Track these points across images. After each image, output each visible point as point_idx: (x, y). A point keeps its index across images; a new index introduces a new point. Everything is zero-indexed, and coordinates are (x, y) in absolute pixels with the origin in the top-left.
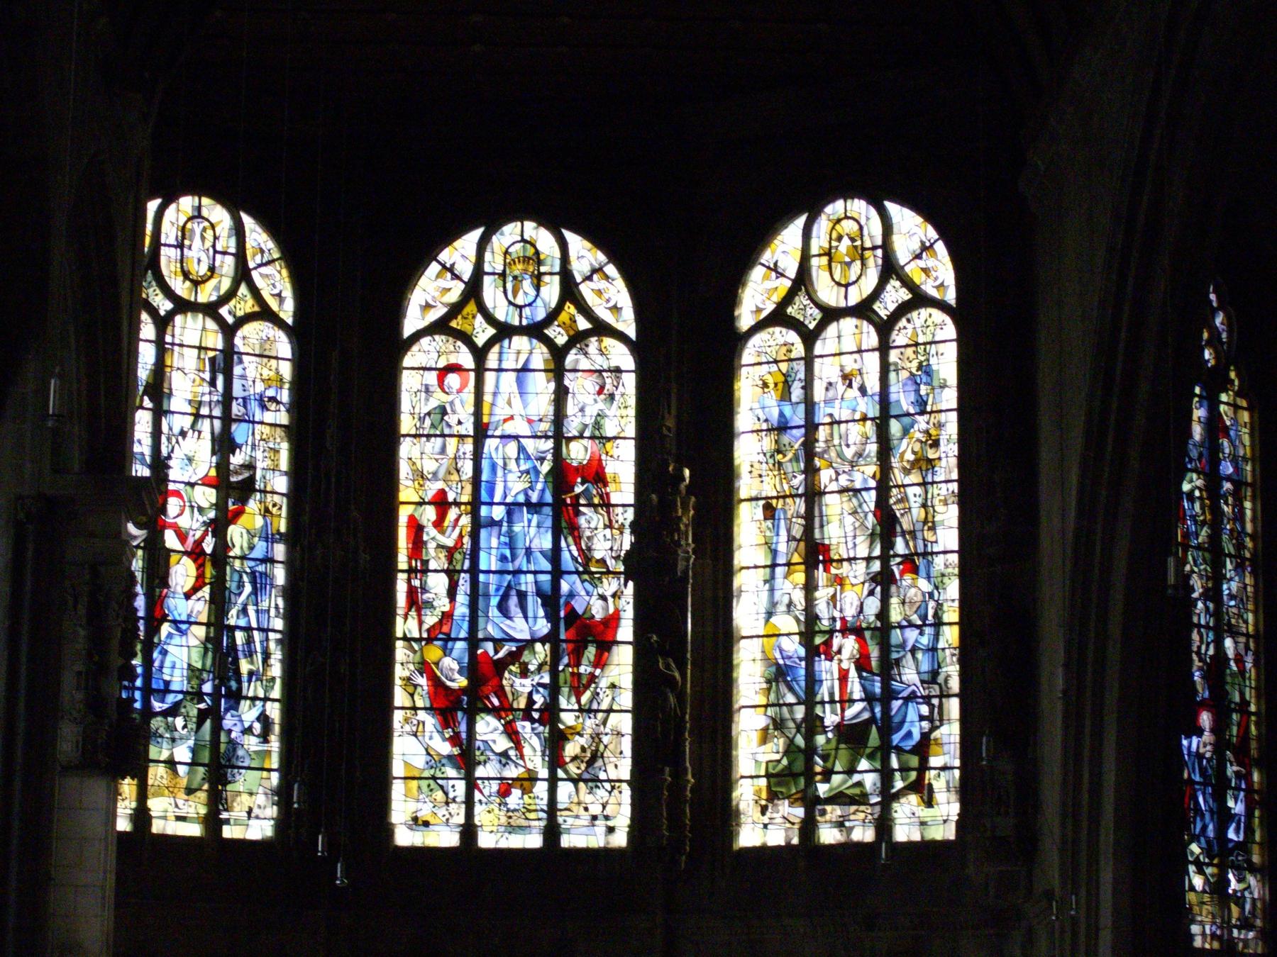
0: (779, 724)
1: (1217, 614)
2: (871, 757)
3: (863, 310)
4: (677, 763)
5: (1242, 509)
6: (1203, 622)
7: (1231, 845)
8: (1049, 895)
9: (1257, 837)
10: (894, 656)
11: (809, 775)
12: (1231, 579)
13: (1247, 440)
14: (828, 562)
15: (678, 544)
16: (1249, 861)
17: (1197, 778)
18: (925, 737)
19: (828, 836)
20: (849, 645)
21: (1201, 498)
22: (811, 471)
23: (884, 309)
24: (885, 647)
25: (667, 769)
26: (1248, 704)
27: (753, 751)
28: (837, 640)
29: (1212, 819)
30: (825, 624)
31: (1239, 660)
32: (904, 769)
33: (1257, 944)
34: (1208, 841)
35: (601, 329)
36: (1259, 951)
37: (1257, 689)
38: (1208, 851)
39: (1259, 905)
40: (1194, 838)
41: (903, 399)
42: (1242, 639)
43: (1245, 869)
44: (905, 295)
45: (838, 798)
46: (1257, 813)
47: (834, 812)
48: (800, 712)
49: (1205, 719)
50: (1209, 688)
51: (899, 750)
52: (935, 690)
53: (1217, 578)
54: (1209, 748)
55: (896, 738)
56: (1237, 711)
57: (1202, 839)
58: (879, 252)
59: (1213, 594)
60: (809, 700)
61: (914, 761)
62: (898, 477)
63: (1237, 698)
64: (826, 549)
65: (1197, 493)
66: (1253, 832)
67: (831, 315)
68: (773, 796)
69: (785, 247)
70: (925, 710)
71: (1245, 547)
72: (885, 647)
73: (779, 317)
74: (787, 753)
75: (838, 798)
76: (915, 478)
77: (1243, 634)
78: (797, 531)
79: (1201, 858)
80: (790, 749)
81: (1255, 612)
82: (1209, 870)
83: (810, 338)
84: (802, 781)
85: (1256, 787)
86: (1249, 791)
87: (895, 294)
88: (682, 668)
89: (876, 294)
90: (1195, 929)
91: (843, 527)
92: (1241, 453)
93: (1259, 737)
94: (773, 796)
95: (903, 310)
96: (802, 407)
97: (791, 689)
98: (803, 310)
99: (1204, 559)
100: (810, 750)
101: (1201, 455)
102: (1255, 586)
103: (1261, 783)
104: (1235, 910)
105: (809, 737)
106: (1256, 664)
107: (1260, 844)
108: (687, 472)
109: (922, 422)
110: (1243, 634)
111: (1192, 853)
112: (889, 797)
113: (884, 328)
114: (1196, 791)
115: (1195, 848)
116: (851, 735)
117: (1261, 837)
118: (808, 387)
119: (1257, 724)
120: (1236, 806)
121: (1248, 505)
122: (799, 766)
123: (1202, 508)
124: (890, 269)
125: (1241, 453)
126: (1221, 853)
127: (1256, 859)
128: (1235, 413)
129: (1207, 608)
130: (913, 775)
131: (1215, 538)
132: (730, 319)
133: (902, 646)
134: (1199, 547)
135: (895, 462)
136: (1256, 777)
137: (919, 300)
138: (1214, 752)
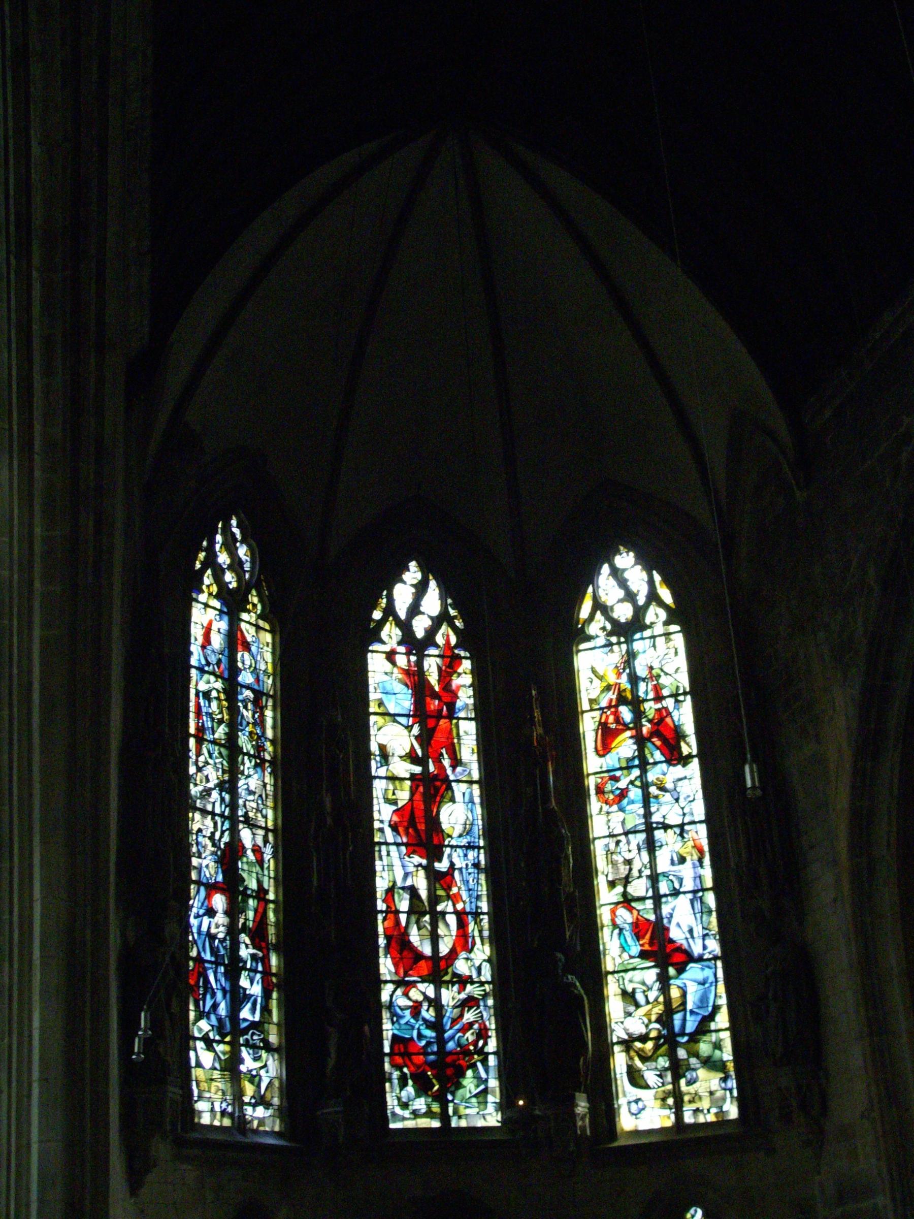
5: (262, 716)
6: (218, 811)
7: (244, 1025)
9: (275, 1018)
12: (249, 776)
13: (269, 657)
16: (265, 1041)
17: (207, 956)
21: (218, 698)
26: (267, 892)
29: (224, 997)
33: (274, 1122)
34: (220, 1020)
36: (277, 1129)
37: (275, 879)
38: (220, 1028)
39: (276, 1083)
40: (201, 1015)
42: (261, 832)
43: (262, 1048)
46: (275, 995)
50: (223, 872)
54: (222, 929)
56: (254, 898)
57: (213, 1017)
59: (229, 785)
65: (214, 694)
66: (270, 1012)
71: (264, 750)
77: (260, 827)
79: (211, 1035)
81: (275, 809)
82: (220, 1048)
85: (274, 970)
86: (266, 973)
90: (201, 1106)
92: (262, 667)
93: (277, 924)
99: (220, 753)
101: (219, 662)
102: (275, 785)
103: (278, 967)
106: (275, 855)
107: (278, 1025)
110: (260, 827)
111: (200, 1030)
114: (205, 969)
115: (204, 1025)
117: (279, 1017)
119: (276, 911)
121: (269, 713)
123: (220, 707)
125: (263, 667)
126: (231, 1030)
127: (273, 1039)
128: (257, 632)
129: (223, 800)
134: (214, 742)
136: (274, 960)
138: (227, 934)
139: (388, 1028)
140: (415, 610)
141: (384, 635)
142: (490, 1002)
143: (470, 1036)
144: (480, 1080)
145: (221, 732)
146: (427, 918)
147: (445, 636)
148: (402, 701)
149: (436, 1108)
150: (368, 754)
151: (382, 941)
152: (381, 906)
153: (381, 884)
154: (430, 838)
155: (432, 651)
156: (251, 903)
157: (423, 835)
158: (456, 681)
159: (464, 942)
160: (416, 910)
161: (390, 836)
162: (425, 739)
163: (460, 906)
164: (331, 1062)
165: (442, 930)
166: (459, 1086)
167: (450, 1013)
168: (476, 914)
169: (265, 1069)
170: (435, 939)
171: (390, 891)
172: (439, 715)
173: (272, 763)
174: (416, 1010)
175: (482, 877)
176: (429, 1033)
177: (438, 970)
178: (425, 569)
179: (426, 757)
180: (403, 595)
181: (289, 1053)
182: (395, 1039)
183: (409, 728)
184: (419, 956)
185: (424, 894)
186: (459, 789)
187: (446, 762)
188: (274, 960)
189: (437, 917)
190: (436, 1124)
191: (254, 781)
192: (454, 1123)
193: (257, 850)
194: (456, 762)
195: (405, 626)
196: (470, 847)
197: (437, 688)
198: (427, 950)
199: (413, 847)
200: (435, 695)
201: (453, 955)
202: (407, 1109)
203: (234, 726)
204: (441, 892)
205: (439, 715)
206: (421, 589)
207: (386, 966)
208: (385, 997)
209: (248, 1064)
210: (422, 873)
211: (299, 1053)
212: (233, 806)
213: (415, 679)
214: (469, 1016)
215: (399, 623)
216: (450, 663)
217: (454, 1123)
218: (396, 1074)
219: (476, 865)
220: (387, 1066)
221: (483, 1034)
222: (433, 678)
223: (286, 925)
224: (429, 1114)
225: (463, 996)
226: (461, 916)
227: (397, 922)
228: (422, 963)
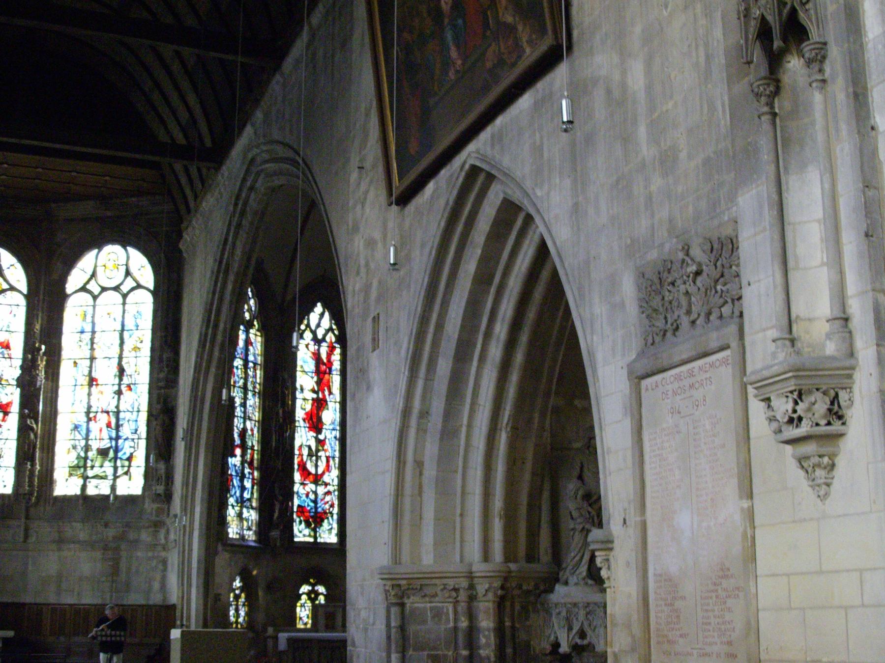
0: (74, 447)
1: (245, 412)
2: (110, 461)
3: (116, 289)
4: (33, 460)
8: (176, 516)
9: (255, 495)
10: (121, 423)
11: (85, 467)
13: (259, 348)
14: (97, 385)
15: (38, 375)
17: (234, 473)
18: (132, 454)
19: (91, 491)
20: (103, 419)
22: (92, 349)
23: (125, 289)
24: (118, 419)
25: (29, 463)
27: (64, 456)
28: (99, 415)
30: (93, 410)
31: (252, 430)
32: (123, 466)
35: (12, 288)
38: (237, 502)
40: (231, 496)
41: (129, 325)
44: (135, 284)
45: (96, 477)
47: (94, 482)
48: (83, 443)
49: (238, 451)
51: (121, 459)
52: (136, 436)
53: (245, 398)
55: (120, 455)
58: (125, 267)
60: (87, 439)
61: (127, 463)
62: (125, 354)
63: (250, 444)
64: (96, 380)
67: (104, 289)
68: (71, 475)
69: (87, 261)
70: (132, 444)
72: (118, 419)
73: (83, 289)
74: (77, 458)
75: (96, 477)
76: (133, 354)
78: (87, 373)
80: (79, 457)
83: (95, 298)
84: (82, 470)
86: (253, 479)
87: (130, 283)
88: (37, 423)
89: (121, 284)
90: (230, 530)
91: (106, 372)
94: (71, 475)
95: (133, 289)
96: (91, 325)
97: (79, 432)
98: (93, 287)
100: (86, 458)
104: (245, 523)
105: (86, 451)
106: (258, 432)
108: (43, 347)
109: (137, 334)
112: (116, 477)
113: (125, 296)
116: (103, 453)
118: (93, 317)
120: (248, 484)
122: (82, 464)
124: (128, 273)
126: (241, 501)
127: (254, 504)
130: (126, 469)
131: (245, 384)
132: (64, 289)
133: (124, 419)
135: (125, 347)
137: (139, 286)
139: (296, 502)
140: (318, 325)
141: (305, 336)
142: (336, 493)
143: (327, 506)
144: (329, 524)
145: (242, 382)
146: (314, 458)
147: (330, 337)
148: (311, 366)
149: (312, 534)
150: (296, 389)
151: (296, 467)
152: (297, 452)
153: (297, 444)
154: (317, 425)
155: (324, 344)
156: (249, 451)
157: (315, 423)
158: (333, 358)
159: (328, 468)
160: (310, 455)
161: (302, 423)
162: (319, 383)
163: (327, 454)
164: (276, 515)
165: (319, 463)
166: (321, 525)
167: (320, 496)
168: (334, 458)
169: (252, 515)
170: (316, 466)
171: (300, 447)
172: (325, 373)
173: (259, 393)
174: (307, 495)
175: (337, 442)
176: (312, 504)
177: (317, 479)
178: (324, 307)
179: (319, 390)
180: (314, 317)
181: (261, 510)
182: (299, 506)
183: (312, 378)
184: (310, 473)
185: (314, 448)
186: (331, 405)
187: (326, 393)
188: (256, 474)
189: (318, 458)
190: (312, 540)
191: (253, 401)
192: (319, 540)
193: (252, 430)
194: (330, 393)
195: (314, 333)
196: (334, 429)
197: (325, 361)
198: (313, 471)
199: (311, 428)
200: (324, 364)
201: (323, 473)
202: (301, 533)
203: (246, 379)
204: (320, 448)
205: (325, 373)
206: (322, 315)
207: (297, 476)
208: (295, 489)
209: (245, 514)
210: (314, 439)
211: (264, 509)
212: (245, 412)
213: (317, 356)
214: (328, 498)
215: (312, 331)
216: (332, 349)
217: (319, 540)
218: (298, 520)
219: (335, 437)
220: (295, 516)
221: (332, 506)
222: (324, 356)
223: (262, 460)
224: (310, 536)
225: (326, 490)
226: (328, 458)
227: (302, 460)
228: (311, 477)
